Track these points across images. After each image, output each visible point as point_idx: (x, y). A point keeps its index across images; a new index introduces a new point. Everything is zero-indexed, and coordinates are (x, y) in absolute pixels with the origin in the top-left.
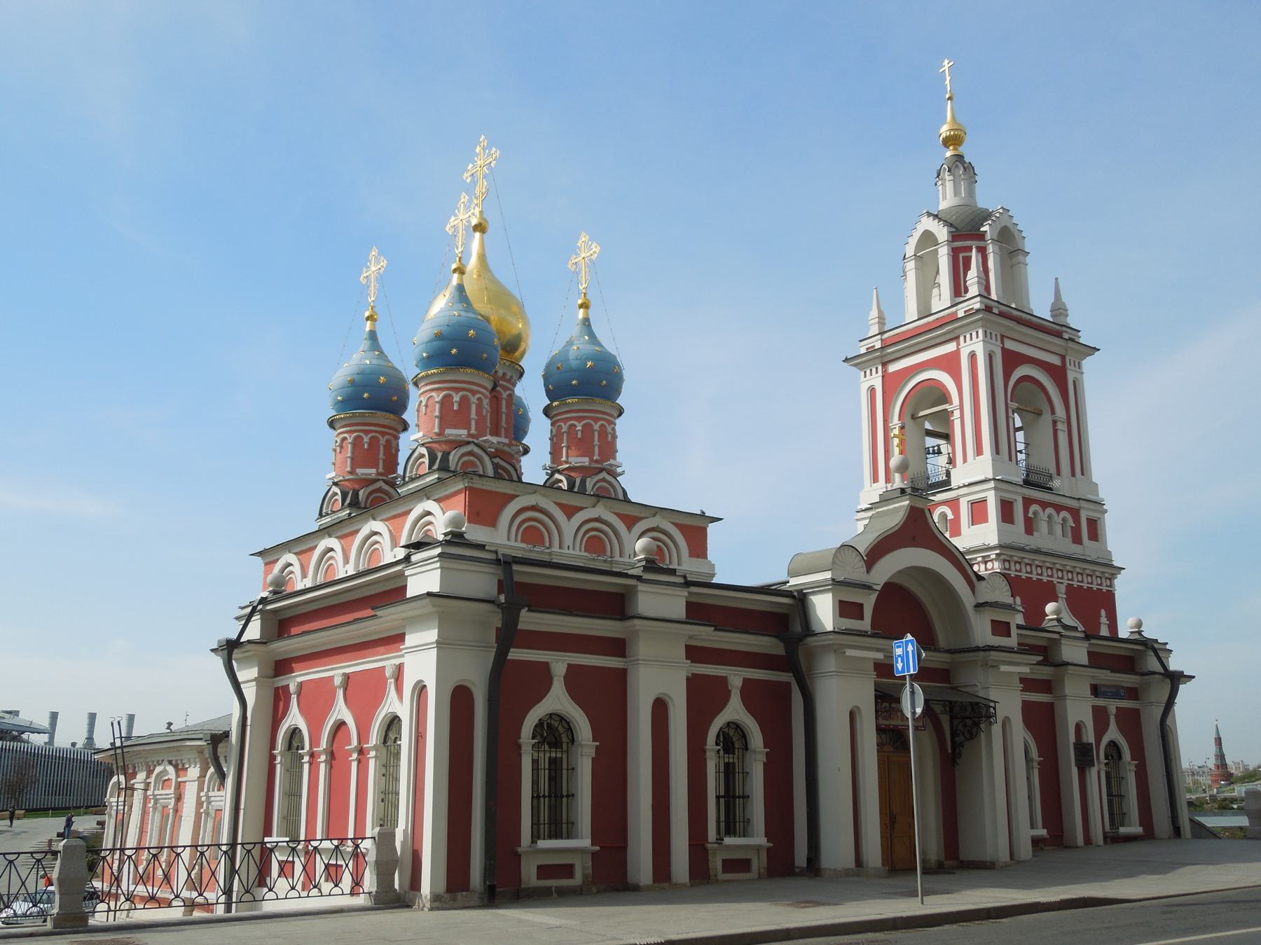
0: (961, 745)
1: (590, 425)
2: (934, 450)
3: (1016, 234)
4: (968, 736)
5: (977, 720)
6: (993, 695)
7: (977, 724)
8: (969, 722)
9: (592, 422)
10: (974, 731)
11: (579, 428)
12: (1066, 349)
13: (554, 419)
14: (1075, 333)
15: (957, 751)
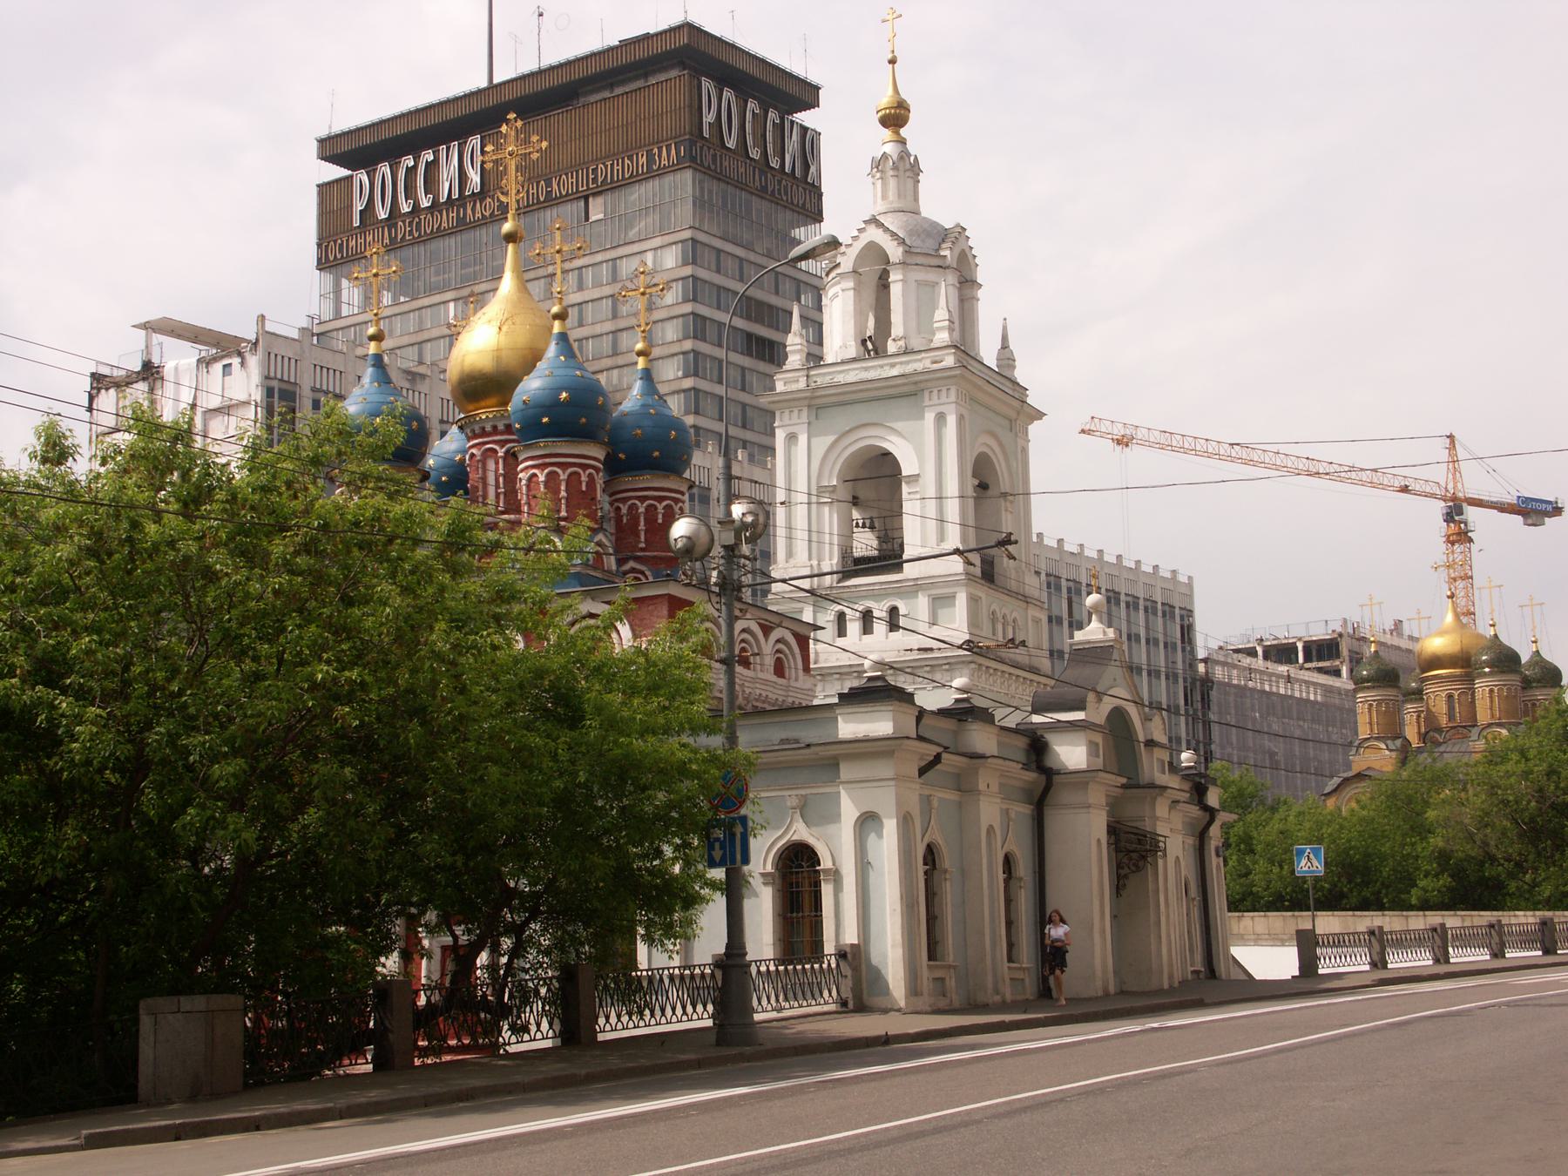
0: (1126, 876)
1: (671, 506)
2: (864, 524)
3: (970, 258)
4: (1133, 868)
5: (1144, 854)
6: (1161, 829)
7: (1144, 858)
8: (1134, 855)
9: (672, 503)
10: (1141, 864)
11: (642, 510)
12: (1018, 413)
13: (614, 497)
14: (1022, 391)
15: (1121, 882)
